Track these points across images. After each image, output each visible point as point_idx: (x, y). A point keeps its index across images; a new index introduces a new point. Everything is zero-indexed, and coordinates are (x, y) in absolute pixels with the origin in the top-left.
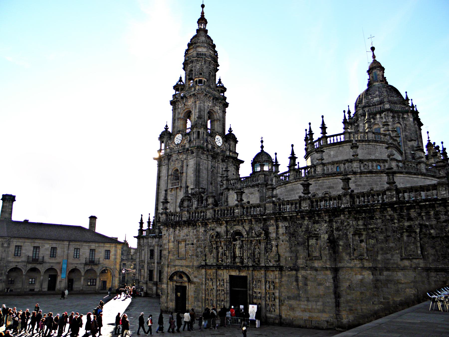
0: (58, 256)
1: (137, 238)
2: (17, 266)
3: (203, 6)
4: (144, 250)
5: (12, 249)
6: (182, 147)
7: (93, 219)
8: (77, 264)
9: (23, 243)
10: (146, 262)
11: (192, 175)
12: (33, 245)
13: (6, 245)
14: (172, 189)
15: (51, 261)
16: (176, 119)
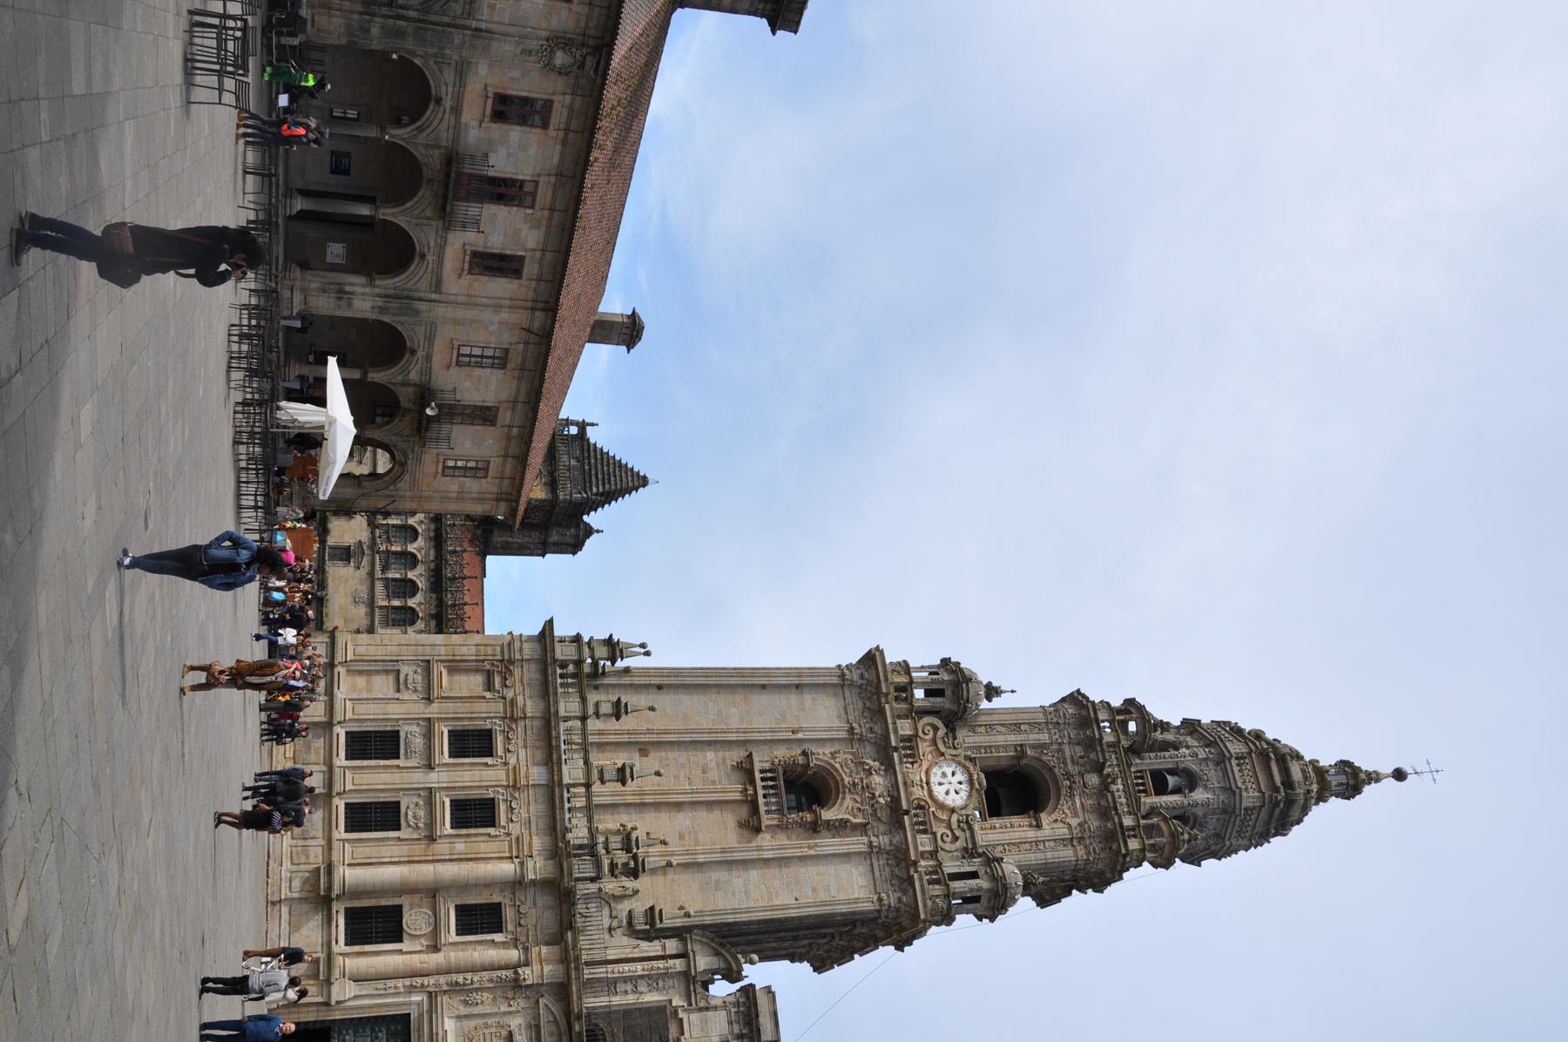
0: (476, 285)
1: (543, 633)
2: (439, 101)
3: (1399, 775)
4: (489, 686)
5: (528, 82)
6: (922, 807)
7: (628, 332)
8: (429, 358)
9: (561, 134)
10: (434, 710)
11: (807, 896)
12: (543, 180)
13: (560, 58)
14: (749, 773)
15: (450, 253)
16: (1020, 731)
